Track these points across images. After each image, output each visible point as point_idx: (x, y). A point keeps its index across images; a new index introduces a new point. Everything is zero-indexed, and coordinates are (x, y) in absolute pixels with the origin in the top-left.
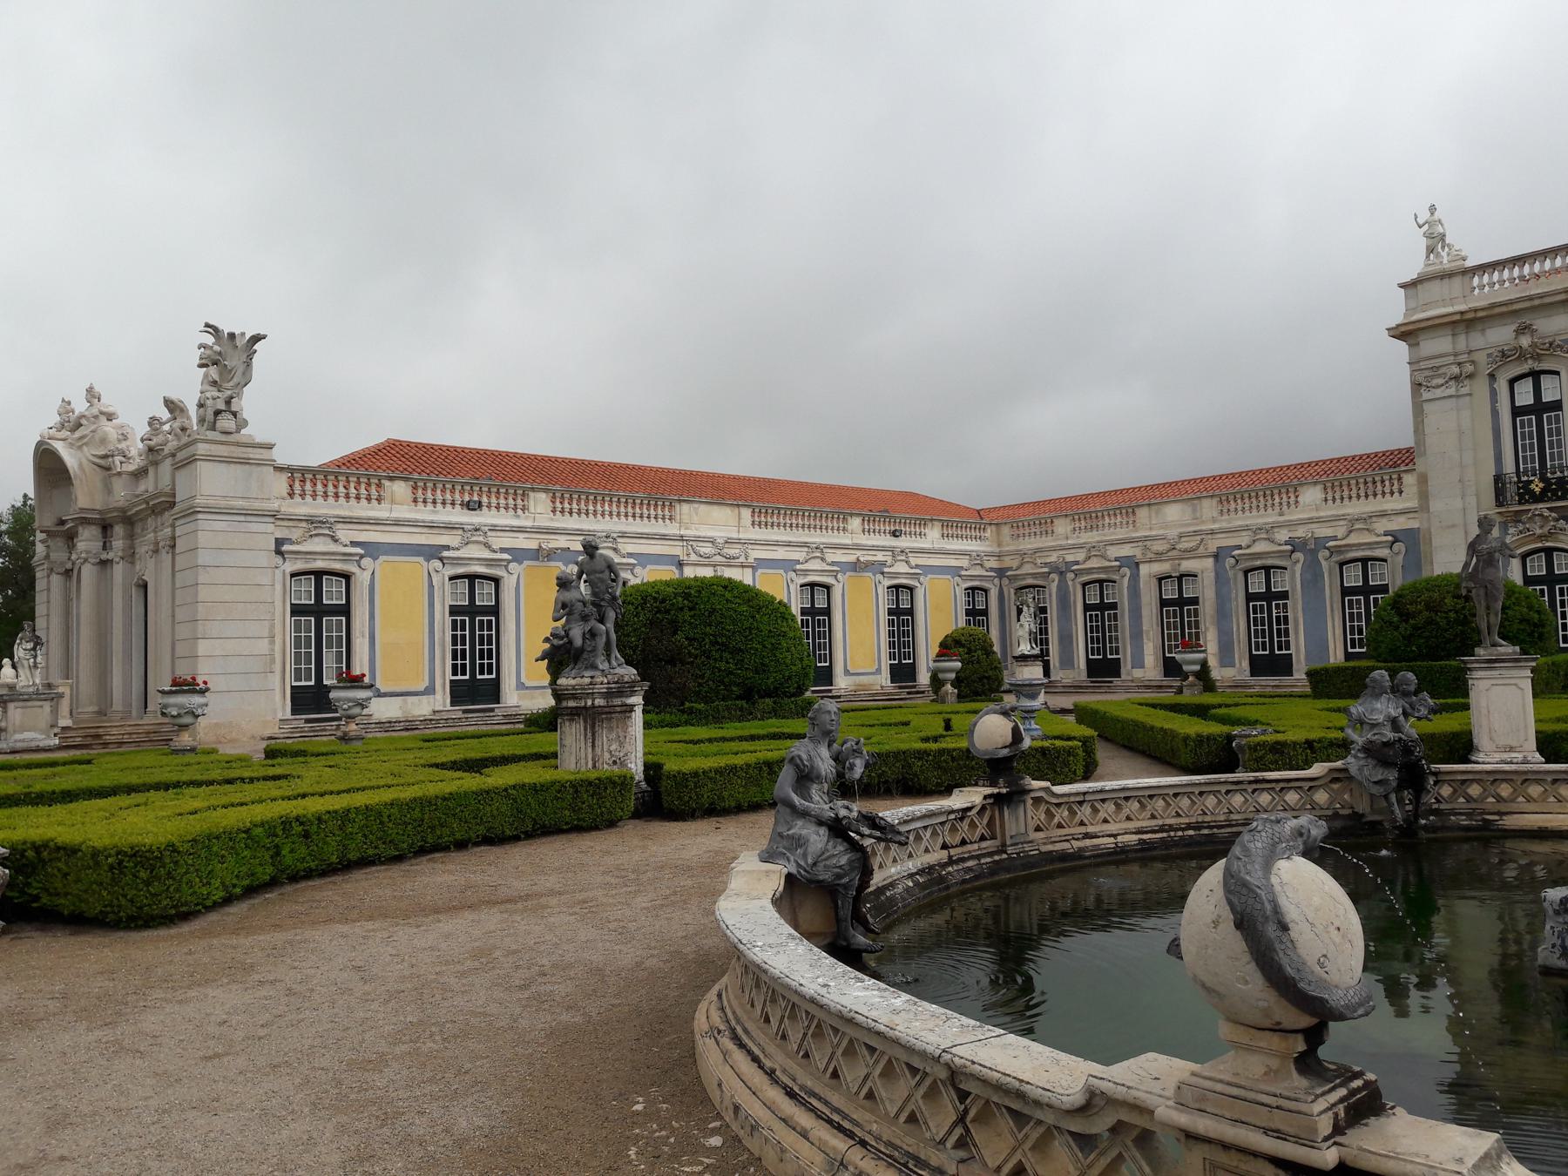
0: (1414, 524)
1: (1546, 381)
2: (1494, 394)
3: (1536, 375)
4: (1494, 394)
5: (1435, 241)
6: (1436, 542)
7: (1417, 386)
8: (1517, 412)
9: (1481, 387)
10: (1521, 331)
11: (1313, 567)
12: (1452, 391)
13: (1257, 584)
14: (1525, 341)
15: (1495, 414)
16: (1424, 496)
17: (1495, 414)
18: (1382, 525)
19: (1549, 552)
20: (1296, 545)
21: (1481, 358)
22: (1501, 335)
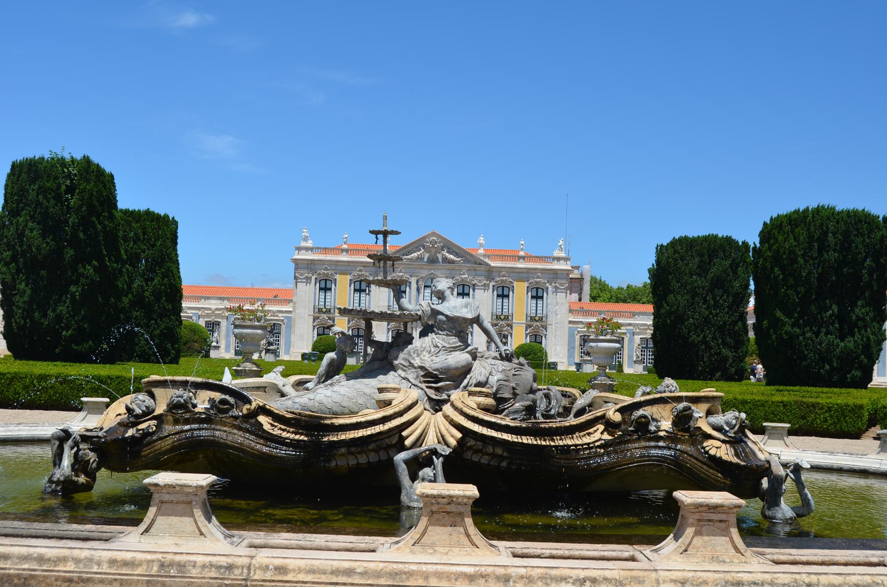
0: (290, 315)
6: (296, 321)
16: (294, 308)
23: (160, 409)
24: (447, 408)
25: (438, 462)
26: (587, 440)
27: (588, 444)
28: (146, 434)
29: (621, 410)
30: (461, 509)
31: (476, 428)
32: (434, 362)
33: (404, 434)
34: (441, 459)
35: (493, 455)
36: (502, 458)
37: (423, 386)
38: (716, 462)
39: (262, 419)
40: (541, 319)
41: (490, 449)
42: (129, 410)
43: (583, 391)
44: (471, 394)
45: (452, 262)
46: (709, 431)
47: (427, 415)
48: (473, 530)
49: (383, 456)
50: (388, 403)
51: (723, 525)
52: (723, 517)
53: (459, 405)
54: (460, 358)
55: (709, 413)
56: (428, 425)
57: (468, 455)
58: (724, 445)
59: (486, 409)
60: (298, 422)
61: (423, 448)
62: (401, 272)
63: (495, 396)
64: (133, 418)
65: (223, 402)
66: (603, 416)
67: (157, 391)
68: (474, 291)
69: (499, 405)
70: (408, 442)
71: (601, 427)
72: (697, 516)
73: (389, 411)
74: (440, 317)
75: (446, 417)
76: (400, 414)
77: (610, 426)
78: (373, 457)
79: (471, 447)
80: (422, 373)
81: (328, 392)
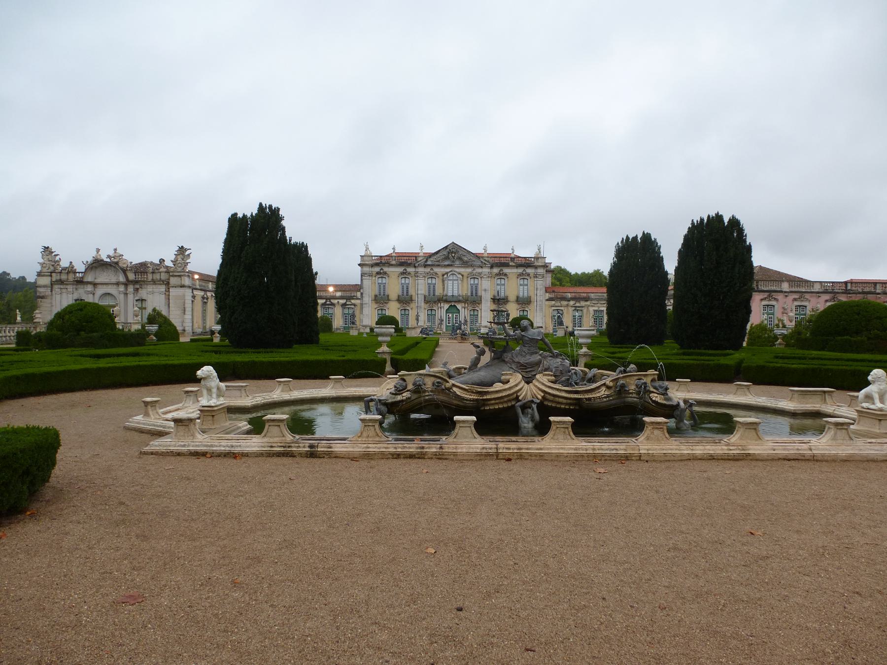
5: (367, 249)
7: (362, 276)
10: (380, 270)
12: (368, 278)
23: (410, 387)
25: (534, 406)
26: (598, 395)
27: (599, 397)
30: (567, 426)
33: (519, 394)
34: (536, 405)
37: (520, 371)
39: (455, 389)
46: (652, 389)
48: (572, 433)
49: (510, 405)
51: (662, 430)
52: (662, 427)
56: (527, 390)
57: (546, 403)
58: (659, 395)
61: (526, 400)
62: (432, 269)
65: (438, 383)
66: (604, 384)
70: (520, 398)
72: (652, 427)
74: (527, 339)
75: (536, 386)
76: (516, 385)
77: (608, 388)
78: (505, 405)
80: (519, 365)
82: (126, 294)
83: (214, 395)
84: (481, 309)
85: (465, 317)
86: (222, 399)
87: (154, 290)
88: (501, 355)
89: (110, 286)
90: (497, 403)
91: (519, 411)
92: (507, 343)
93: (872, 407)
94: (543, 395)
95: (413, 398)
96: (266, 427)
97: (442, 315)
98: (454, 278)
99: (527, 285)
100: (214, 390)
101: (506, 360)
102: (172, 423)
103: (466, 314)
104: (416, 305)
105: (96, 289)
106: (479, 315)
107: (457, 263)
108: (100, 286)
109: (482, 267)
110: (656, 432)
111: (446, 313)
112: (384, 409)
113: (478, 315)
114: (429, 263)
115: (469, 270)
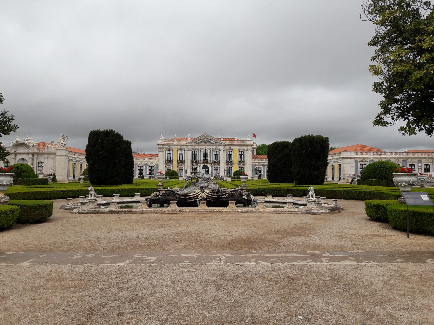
1: (170, 152)
2: (166, 152)
3: (169, 151)
4: (166, 152)
8: (167, 154)
9: (164, 151)
11: (146, 167)
13: (139, 168)
14: (169, 148)
15: (166, 154)
17: (166, 154)
18: (154, 163)
19: (169, 167)
20: (144, 164)
21: (165, 148)
22: (167, 147)
24: (204, 192)
28: (160, 198)
29: (230, 192)
31: (209, 195)
32: (203, 185)
35: (211, 199)
36: (212, 199)
38: (244, 199)
39: (176, 195)
40: (243, 162)
41: (211, 198)
42: (156, 195)
43: (228, 189)
44: (208, 190)
45: (212, 143)
47: (201, 193)
48: (206, 205)
49: (195, 200)
50: (196, 192)
53: (206, 192)
54: (207, 184)
55: (244, 192)
59: (211, 192)
60: (182, 195)
62: (195, 147)
63: (212, 190)
64: (157, 196)
67: (160, 192)
68: (220, 152)
69: (213, 191)
70: (199, 198)
71: (228, 194)
73: (196, 193)
74: (203, 178)
76: (197, 193)
77: (229, 194)
78: (194, 200)
79: (208, 198)
81: (186, 191)
82: (33, 159)
83: (93, 196)
84: (220, 167)
85: (212, 171)
86: (95, 198)
87: (48, 157)
88: (195, 184)
89: (24, 155)
90: (190, 200)
91: (198, 202)
92: (198, 179)
93: (310, 199)
94: (206, 196)
95: (162, 198)
96: (111, 205)
97: (200, 171)
98: (206, 151)
99: (243, 154)
100: (93, 195)
101: (196, 185)
102: (80, 204)
103: (212, 169)
104: (187, 165)
105: (16, 156)
106: (219, 170)
107: (208, 143)
108: (19, 155)
109: (220, 146)
110: (232, 205)
111: (202, 168)
112: (152, 202)
113: (218, 170)
114: (193, 143)
115: (214, 147)
